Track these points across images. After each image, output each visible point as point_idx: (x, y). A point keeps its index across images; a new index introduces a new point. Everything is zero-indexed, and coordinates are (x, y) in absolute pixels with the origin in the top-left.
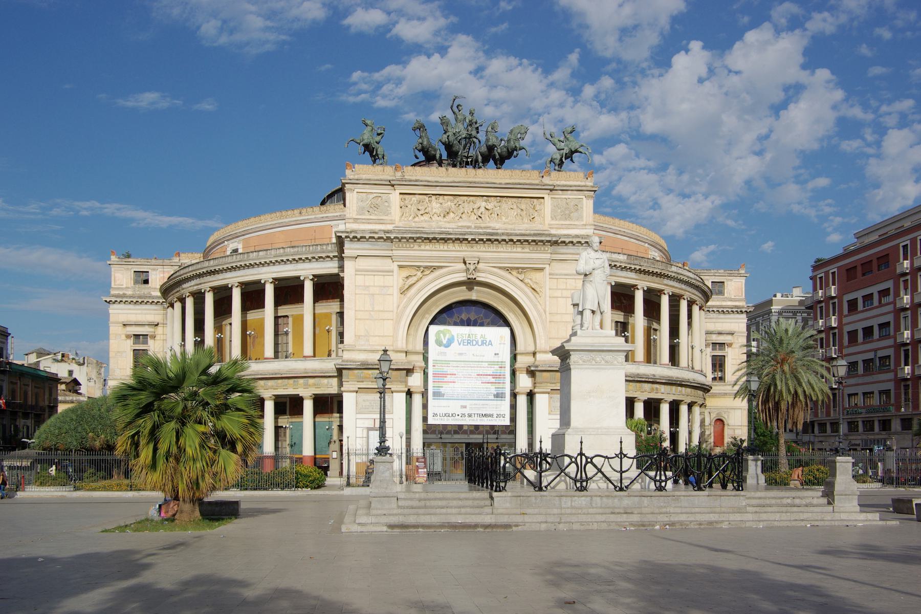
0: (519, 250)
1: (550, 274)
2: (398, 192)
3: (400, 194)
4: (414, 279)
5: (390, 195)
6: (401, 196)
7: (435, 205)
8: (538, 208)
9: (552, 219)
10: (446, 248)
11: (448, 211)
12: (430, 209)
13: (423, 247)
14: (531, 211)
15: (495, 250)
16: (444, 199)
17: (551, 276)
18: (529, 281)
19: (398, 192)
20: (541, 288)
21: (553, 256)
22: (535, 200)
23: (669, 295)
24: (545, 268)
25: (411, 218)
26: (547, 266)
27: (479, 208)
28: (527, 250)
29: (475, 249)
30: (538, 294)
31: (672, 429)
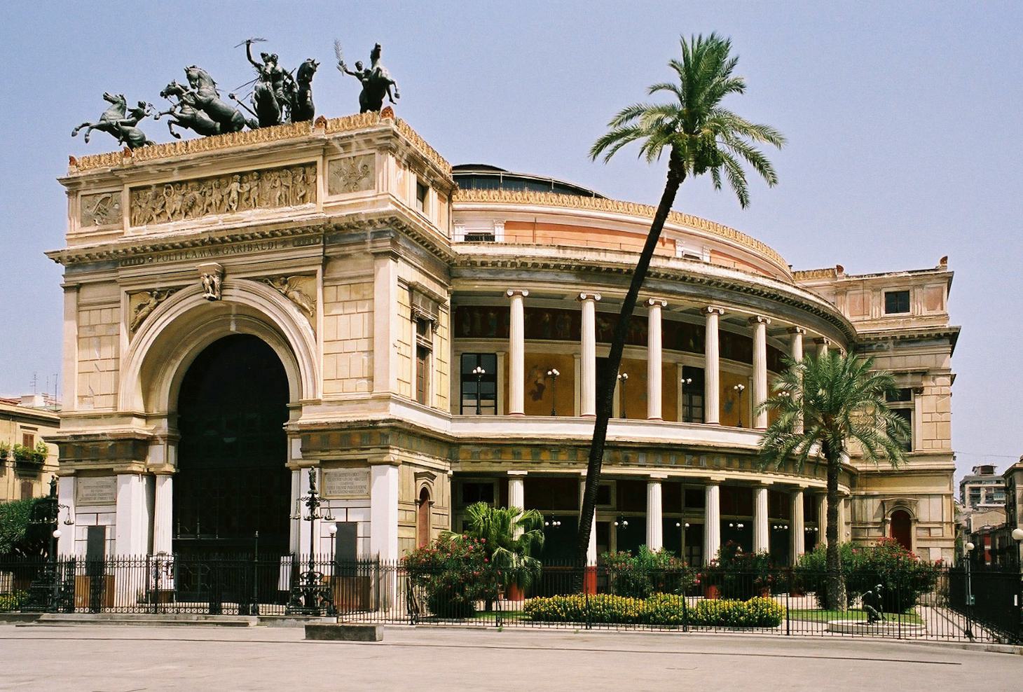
0: (280, 247)
1: (324, 281)
2: (127, 187)
3: (132, 189)
4: (147, 308)
5: (121, 193)
6: (135, 193)
7: (175, 201)
8: (312, 179)
9: (331, 192)
10: (184, 257)
11: (190, 204)
12: (167, 205)
13: (155, 260)
14: (300, 186)
15: (247, 253)
16: (187, 188)
17: (326, 284)
18: (296, 295)
19: (127, 187)
20: (314, 302)
21: (328, 251)
22: (308, 169)
23: (663, 308)
24: (317, 271)
25: (145, 222)
26: (319, 269)
27: (230, 193)
28: (290, 247)
29: (221, 254)
30: (309, 312)
31: (807, 529)
